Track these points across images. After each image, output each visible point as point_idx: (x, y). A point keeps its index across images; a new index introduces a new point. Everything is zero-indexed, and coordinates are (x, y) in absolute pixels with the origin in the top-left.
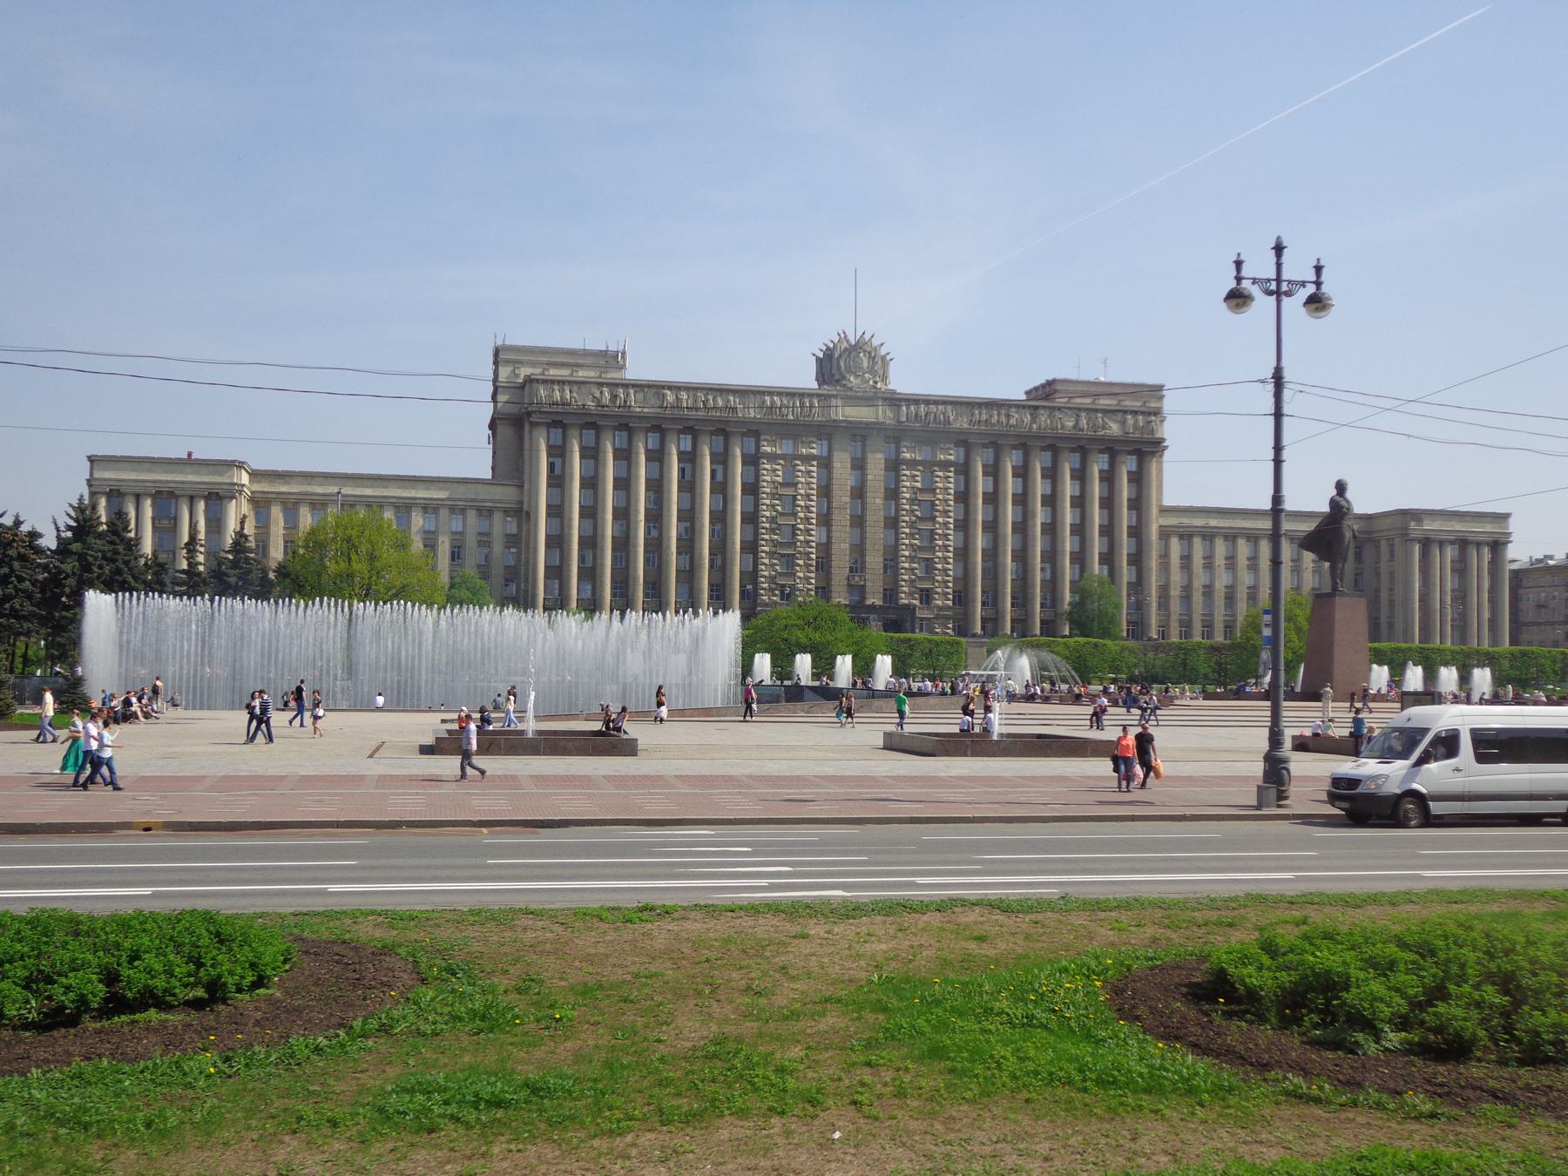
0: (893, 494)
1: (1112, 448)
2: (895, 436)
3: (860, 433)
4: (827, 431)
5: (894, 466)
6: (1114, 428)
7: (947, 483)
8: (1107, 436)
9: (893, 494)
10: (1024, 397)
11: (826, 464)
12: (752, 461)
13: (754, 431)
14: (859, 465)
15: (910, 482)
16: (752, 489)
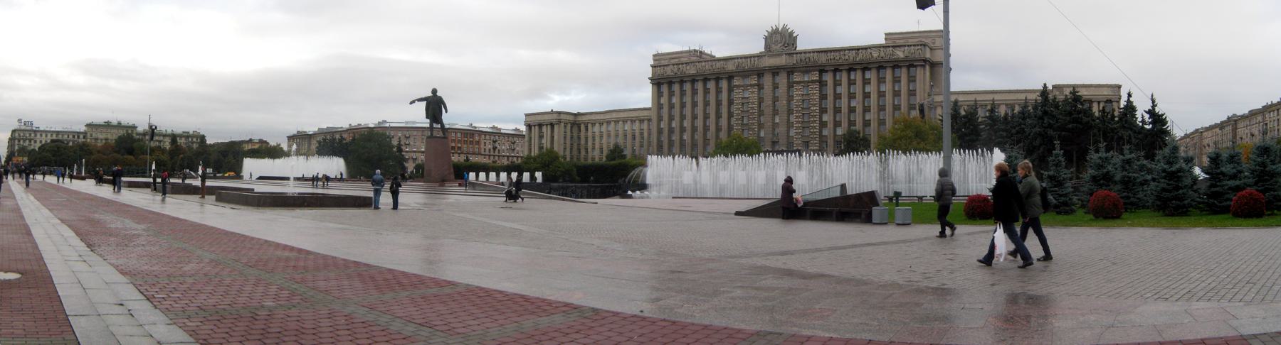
0: (790, 99)
1: (896, 65)
2: (790, 71)
3: (775, 71)
4: (760, 73)
5: (790, 85)
6: (900, 54)
7: (815, 91)
8: (917, 59)
9: (790, 99)
10: (881, 40)
11: (760, 87)
12: (730, 90)
13: (730, 77)
14: (775, 87)
15: (798, 92)
16: (730, 102)
